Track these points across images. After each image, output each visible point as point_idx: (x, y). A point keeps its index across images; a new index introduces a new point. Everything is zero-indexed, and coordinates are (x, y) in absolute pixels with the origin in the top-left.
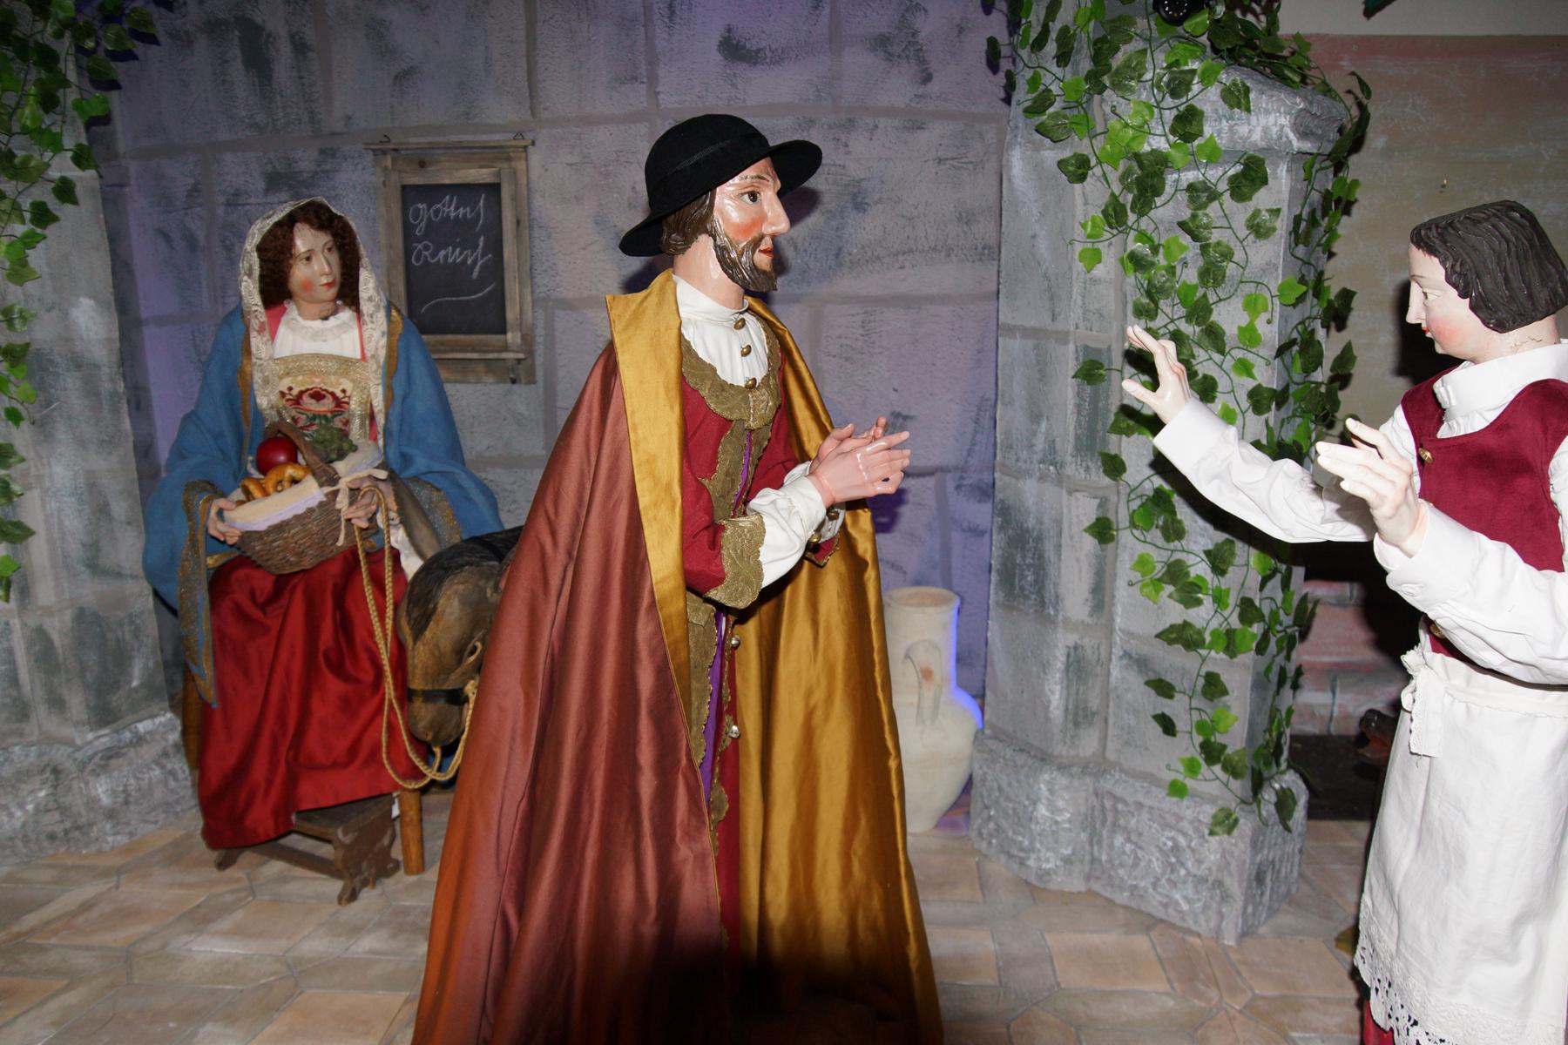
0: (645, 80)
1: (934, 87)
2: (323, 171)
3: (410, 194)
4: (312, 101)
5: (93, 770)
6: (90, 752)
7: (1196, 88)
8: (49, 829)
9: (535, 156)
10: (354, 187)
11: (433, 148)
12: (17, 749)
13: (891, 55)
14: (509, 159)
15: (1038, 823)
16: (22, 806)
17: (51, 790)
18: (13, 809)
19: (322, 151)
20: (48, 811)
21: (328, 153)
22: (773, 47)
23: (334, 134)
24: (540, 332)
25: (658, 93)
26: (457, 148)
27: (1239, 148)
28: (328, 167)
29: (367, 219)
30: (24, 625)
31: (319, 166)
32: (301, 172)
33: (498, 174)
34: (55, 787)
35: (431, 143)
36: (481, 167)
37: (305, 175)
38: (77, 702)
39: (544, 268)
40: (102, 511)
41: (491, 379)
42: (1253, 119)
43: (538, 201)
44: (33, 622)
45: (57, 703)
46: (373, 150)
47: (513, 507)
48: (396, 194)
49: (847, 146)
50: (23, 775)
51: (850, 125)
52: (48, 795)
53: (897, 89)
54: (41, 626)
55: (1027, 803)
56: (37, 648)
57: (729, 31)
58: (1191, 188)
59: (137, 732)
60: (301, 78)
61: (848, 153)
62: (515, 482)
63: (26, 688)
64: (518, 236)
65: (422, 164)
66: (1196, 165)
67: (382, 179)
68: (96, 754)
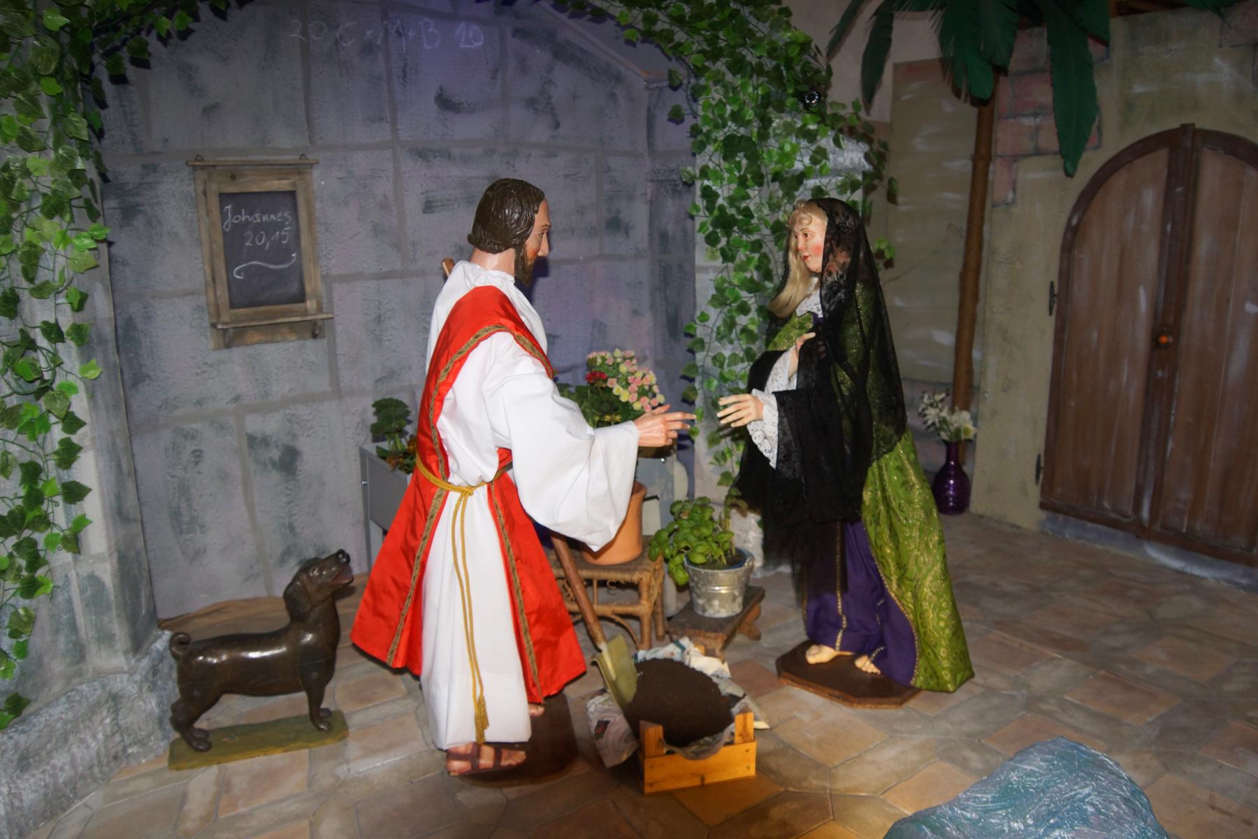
0: (389, 120)
1: (561, 131)
2: (147, 183)
3: (224, 197)
4: (135, 126)
5: (149, 687)
6: (144, 673)
7: (819, 138)
8: (113, 751)
9: (316, 173)
10: (174, 196)
11: (245, 165)
12: (84, 687)
13: (537, 110)
14: (299, 173)
15: (749, 542)
16: (94, 737)
17: (113, 716)
18: (90, 741)
19: (144, 167)
20: (113, 735)
21: (151, 168)
22: (469, 102)
23: (154, 153)
24: (325, 300)
25: (398, 130)
26: (264, 165)
27: (839, 168)
28: (150, 179)
29: (186, 221)
30: (78, 575)
31: (143, 179)
32: (127, 183)
33: (294, 184)
34: (116, 712)
35: (244, 161)
36: (279, 179)
37: (131, 186)
38: (119, 630)
39: (324, 253)
40: (119, 466)
41: (293, 337)
42: (845, 154)
43: (318, 205)
44: (84, 570)
45: (105, 638)
46: (194, 166)
47: (310, 432)
48: (214, 200)
49: (513, 166)
50: (94, 708)
51: (515, 154)
52: (111, 721)
53: (540, 132)
54: (93, 573)
55: (741, 533)
56: (89, 593)
57: (441, 90)
58: (812, 190)
59: (158, 651)
60: (123, 106)
61: (515, 171)
62: (310, 414)
63: (82, 632)
64: (311, 230)
65: (233, 177)
66: (816, 177)
67: (200, 189)
68: (148, 673)
